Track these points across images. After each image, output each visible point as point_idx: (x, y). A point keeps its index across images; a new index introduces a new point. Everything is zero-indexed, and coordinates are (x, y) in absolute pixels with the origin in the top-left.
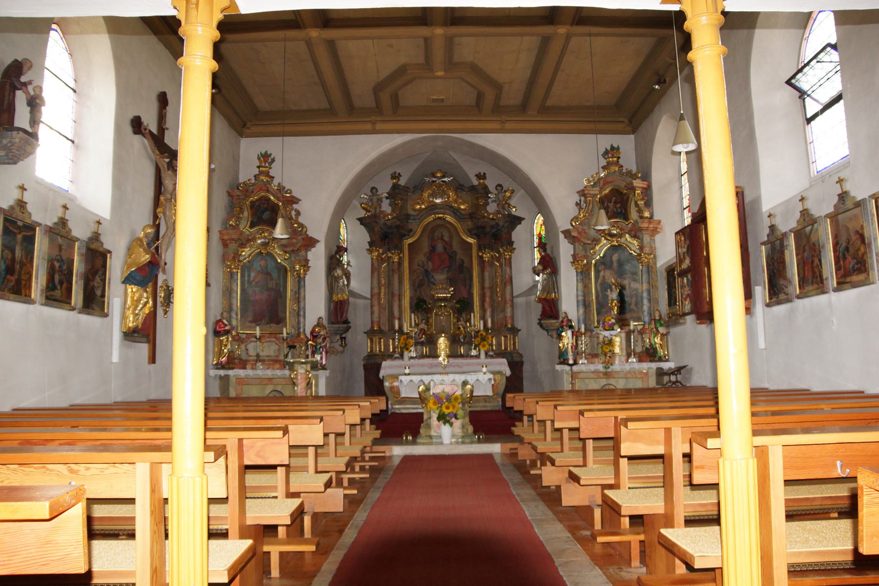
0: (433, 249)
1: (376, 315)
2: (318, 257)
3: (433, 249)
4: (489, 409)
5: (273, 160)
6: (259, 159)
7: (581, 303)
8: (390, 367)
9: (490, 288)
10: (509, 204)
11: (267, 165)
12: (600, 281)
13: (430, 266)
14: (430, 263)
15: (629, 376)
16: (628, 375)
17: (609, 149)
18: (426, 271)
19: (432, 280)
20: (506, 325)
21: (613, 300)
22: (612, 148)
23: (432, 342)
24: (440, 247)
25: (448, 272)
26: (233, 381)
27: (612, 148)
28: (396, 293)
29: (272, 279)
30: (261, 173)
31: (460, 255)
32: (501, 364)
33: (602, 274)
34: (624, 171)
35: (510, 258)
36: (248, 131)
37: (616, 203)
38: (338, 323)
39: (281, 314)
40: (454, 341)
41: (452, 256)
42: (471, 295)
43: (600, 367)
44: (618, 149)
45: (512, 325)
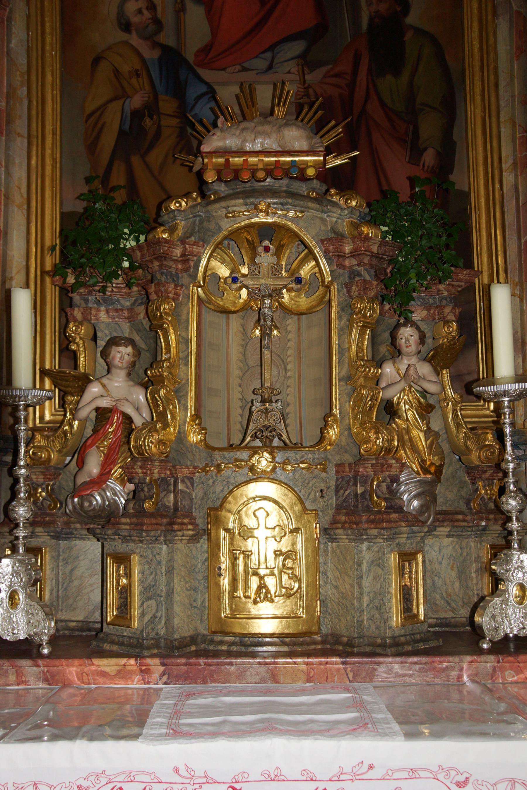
18: (172, 60)
25: (306, 62)
40: (351, 507)
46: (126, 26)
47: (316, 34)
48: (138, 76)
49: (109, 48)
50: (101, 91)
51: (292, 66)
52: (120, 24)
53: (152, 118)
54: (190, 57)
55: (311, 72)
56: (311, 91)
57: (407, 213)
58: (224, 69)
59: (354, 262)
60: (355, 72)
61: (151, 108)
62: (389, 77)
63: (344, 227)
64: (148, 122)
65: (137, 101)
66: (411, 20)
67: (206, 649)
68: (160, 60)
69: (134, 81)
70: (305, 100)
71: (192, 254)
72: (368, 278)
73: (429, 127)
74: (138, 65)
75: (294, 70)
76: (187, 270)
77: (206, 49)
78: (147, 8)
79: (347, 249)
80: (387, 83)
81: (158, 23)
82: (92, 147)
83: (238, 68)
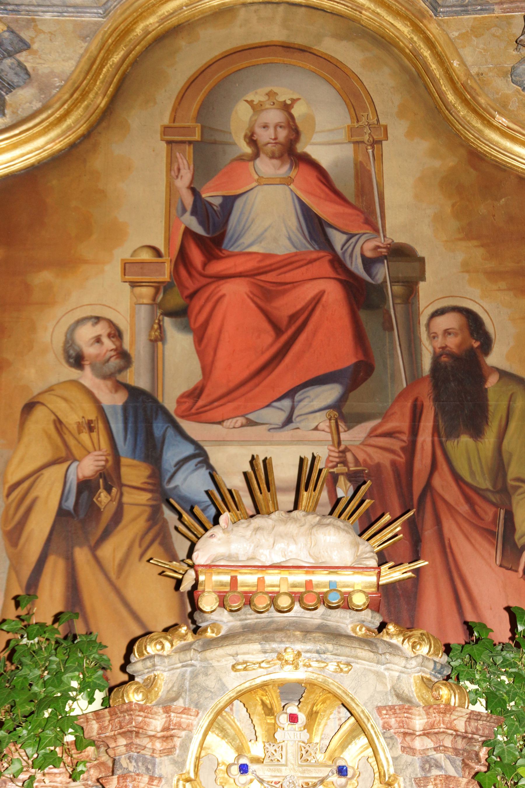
0: (209, 231)
3: (209, 231)
13: (180, 362)
14: (179, 344)
18: (143, 408)
24: (268, 218)
25: (342, 414)
41: (378, 289)
46: (77, 361)
48: (91, 429)
49: (50, 390)
51: (322, 420)
52: (68, 357)
53: (108, 490)
54: (170, 404)
55: (349, 428)
56: (349, 457)
57: (506, 663)
58: (220, 423)
59: (429, 743)
60: (414, 431)
61: (109, 477)
62: (465, 439)
63: (411, 687)
64: (103, 498)
65: (88, 466)
66: (493, 359)
68: (125, 408)
69: (85, 437)
70: (341, 468)
71: (179, 726)
72: (452, 772)
74: (92, 415)
75: (324, 425)
76: (169, 752)
77: (196, 393)
78: (109, 336)
79: (419, 722)
80: (463, 448)
81: (124, 356)
83: (240, 420)
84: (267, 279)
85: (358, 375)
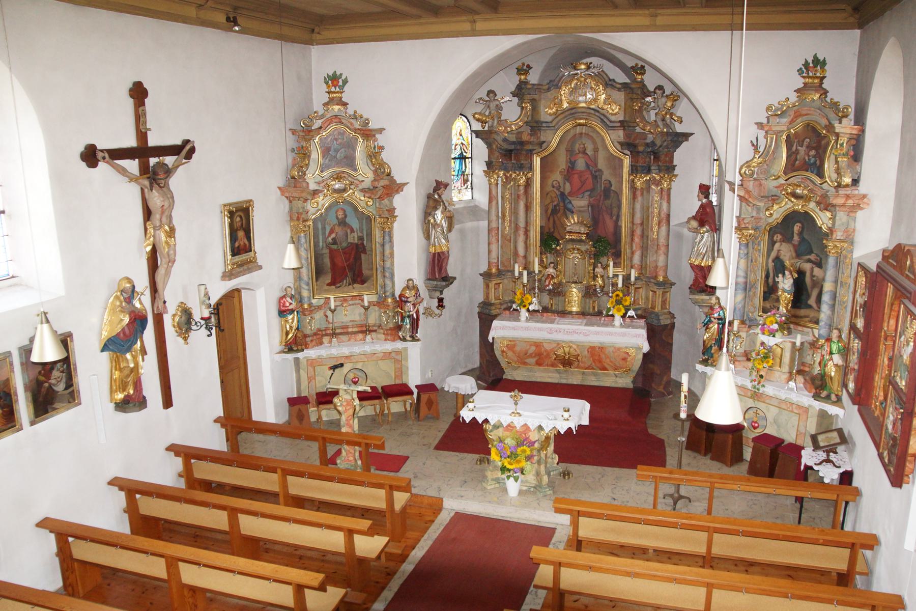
1: (494, 255)
2: (408, 206)
4: (620, 386)
5: (345, 82)
6: (327, 83)
7: (741, 286)
8: (502, 328)
9: (642, 224)
10: (671, 114)
11: (338, 89)
12: (773, 255)
14: (568, 185)
15: (784, 406)
16: (785, 405)
17: (810, 61)
18: (562, 194)
19: (570, 206)
20: (656, 277)
21: (784, 291)
22: (816, 61)
23: (558, 292)
24: (581, 164)
25: (590, 196)
26: (304, 363)
27: (816, 61)
28: (522, 224)
29: (352, 231)
30: (331, 99)
31: (607, 175)
32: (637, 336)
33: (777, 246)
34: (828, 99)
35: (669, 189)
36: (318, 37)
37: (809, 147)
38: (436, 279)
39: (365, 272)
40: (589, 293)
41: (596, 175)
42: (617, 228)
43: (749, 385)
44: (824, 63)
45: (665, 277)
46: (553, 187)
47: (592, 190)
50: (548, 201)
61: (558, 205)
65: (555, 203)
66: (613, 188)
67: (563, 313)
73: (615, 211)
82: (546, 211)
84: (581, 174)
85: (592, 190)
